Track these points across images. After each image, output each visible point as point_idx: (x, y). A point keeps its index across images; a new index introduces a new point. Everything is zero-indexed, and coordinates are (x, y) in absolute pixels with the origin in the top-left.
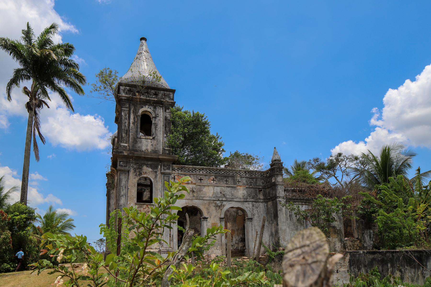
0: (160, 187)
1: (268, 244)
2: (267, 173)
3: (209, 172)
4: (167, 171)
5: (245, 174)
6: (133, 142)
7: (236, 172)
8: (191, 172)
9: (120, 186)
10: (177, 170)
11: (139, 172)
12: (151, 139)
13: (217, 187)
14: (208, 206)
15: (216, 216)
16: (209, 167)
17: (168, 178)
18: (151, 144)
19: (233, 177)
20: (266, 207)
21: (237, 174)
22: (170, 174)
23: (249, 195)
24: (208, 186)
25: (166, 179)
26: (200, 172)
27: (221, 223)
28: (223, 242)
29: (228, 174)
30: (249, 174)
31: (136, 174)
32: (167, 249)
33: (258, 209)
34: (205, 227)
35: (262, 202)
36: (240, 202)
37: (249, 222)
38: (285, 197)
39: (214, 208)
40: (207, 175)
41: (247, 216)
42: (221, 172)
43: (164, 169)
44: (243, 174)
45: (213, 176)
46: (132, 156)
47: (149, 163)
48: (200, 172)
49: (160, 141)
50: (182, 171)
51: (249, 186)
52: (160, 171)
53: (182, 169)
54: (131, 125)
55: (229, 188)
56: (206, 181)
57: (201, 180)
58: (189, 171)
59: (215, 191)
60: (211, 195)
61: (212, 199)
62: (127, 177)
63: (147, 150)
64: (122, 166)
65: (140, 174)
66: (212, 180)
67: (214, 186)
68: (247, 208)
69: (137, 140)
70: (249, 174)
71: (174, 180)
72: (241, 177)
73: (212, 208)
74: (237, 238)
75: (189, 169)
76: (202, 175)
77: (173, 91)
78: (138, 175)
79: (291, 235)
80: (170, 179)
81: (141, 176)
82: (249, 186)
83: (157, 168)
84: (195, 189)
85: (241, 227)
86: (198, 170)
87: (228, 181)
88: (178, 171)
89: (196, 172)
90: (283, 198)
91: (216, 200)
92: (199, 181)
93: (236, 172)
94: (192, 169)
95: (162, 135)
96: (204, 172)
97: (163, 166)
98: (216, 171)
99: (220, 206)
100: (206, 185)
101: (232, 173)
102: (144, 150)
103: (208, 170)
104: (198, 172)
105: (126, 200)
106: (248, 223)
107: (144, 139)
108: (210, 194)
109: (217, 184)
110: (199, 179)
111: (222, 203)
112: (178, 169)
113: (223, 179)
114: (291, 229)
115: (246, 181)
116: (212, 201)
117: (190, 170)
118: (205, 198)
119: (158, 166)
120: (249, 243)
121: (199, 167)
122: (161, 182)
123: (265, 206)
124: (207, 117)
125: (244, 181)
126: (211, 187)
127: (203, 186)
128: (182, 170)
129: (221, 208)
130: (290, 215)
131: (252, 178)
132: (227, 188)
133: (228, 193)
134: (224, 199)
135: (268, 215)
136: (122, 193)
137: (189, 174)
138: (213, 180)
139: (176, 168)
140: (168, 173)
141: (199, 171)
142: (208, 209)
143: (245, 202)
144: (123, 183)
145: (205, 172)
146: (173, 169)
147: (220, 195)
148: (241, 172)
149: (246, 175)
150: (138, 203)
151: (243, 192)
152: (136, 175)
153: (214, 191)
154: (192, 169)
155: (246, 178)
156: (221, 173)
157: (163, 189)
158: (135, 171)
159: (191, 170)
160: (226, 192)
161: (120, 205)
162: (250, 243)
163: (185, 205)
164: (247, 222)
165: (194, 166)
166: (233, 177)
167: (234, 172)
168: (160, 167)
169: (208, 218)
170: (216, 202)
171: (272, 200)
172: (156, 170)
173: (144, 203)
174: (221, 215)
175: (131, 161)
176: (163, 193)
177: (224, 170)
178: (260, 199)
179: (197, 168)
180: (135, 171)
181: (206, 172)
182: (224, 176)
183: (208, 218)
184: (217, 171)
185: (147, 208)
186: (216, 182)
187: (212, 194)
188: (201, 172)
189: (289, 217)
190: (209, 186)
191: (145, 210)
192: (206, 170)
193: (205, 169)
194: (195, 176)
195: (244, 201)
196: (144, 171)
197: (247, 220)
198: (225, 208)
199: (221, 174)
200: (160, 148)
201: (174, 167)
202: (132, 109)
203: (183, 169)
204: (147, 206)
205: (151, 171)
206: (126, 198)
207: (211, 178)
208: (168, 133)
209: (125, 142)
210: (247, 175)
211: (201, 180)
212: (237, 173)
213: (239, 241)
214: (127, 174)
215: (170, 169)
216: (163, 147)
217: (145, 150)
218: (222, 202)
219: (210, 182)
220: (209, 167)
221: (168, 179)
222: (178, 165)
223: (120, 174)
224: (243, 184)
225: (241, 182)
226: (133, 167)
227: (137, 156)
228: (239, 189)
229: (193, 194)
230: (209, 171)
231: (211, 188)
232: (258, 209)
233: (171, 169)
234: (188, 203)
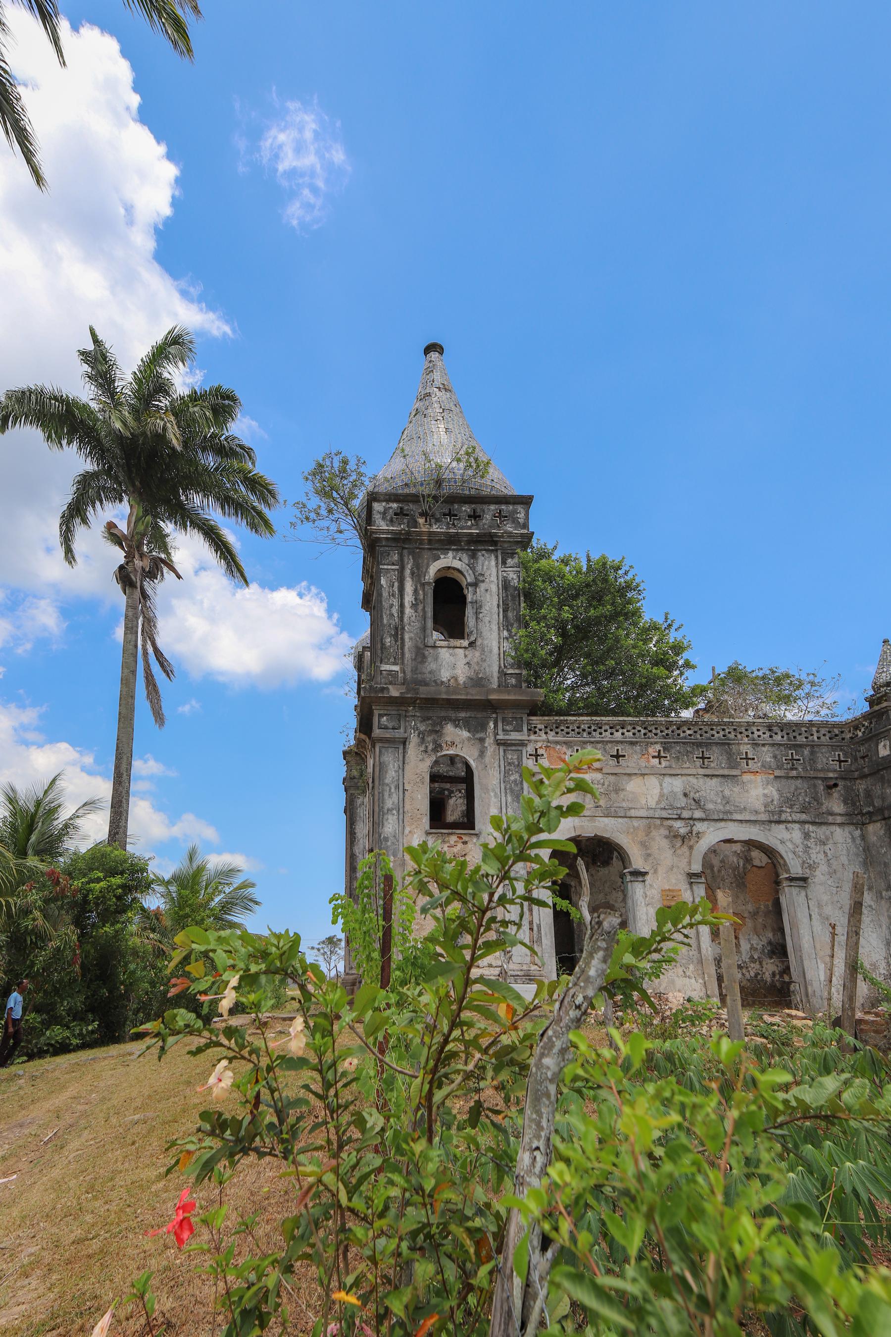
0: (495, 782)
2: (856, 728)
4: (515, 736)
5: (768, 734)
6: (415, 659)
7: (735, 730)
8: (585, 734)
9: (383, 784)
11: (435, 742)
12: (465, 648)
13: (673, 778)
14: (647, 836)
18: (465, 661)
19: (725, 744)
21: (739, 736)
22: (522, 744)
23: (789, 802)
24: (643, 775)
28: (704, 951)
29: (708, 735)
30: (784, 733)
31: (427, 747)
36: (755, 821)
37: (795, 891)
39: (665, 843)
40: (637, 742)
41: (788, 871)
43: (503, 730)
44: (760, 733)
45: (656, 743)
46: (411, 698)
47: (463, 715)
49: (491, 651)
50: (557, 733)
51: (788, 773)
52: (492, 738)
53: (557, 728)
54: (408, 611)
55: (715, 780)
56: (634, 760)
57: (617, 756)
58: (579, 733)
59: (665, 791)
60: (652, 803)
62: (401, 759)
63: (456, 679)
64: (386, 728)
65: (438, 747)
67: (661, 775)
68: (782, 842)
69: (427, 653)
70: (784, 733)
72: (755, 745)
73: (660, 842)
74: (754, 942)
75: (578, 728)
76: (622, 742)
77: (526, 501)
78: (433, 750)
80: (524, 759)
81: (439, 754)
82: (788, 773)
83: (483, 727)
85: (767, 906)
86: (607, 727)
87: (709, 758)
88: (546, 733)
89: (601, 734)
91: (671, 816)
92: (613, 762)
93: (735, 730)
94: (589, 728)
95: (495, 635)
96: (627, 734)
99: (683, 838)
100: (637, 772)
101: (722, 733)
102: (444, 679)
104: (608, 734)
105: (401, 822)
106: (791, 894)
107: (445, 649)
108: (650, 799)
109: (670, 767)
110: (612, 756)
111: (692, 826)
112: (546, 727)
113: (691, 752)
115: (775, 757)
116: (658, 822)
117: (584, 730)
118: (633, 811)
119: (488, 723)
120: (802, 961)
121: (610, 718)
122: (497, 768)
124: (631, 567)
125: (767, 755)
126: (652, 777)
127: (625, 774)
128: (558, 730)
129: (691, 843)
131: (798, 747)
132: (708, 780)
133: (712, 796)
134: (698, 814)
136: (389, 803)
137: (581, 741)
138: (659, 757)
139: (539, 726)
141: (609, 731)
142: (644, 845)
143: (773, 825)
144: (391, 774)
145: (630, 734)
146: (530, 730)
147: (682, 802)
148: (755, 729)
149: (771, 736)
150: (433, 831)
151: (766, 791)
152: (426, 751)
153: (662, 789)
155: (773, 745)
157: (505, 789)
158: (423, 739)
160: (702, 793)
161: (384, 837)
162: (806, 963)
164: (786, 889)
165: (594, 718)
166: (725, 744)
167: (727, 731)
168: (492, 726)
171: (884, 819)
172: (482, 735)
173: (450, 831)
174: (689, 863)
175: (411, 714)
177: (693, 725)
180: (423, 739)
182: (693, 743)
185: (460, 846)
186: (668, 763)
187: (656, 798)
188: (618, 735)
191: (455, 850)
193: (630, 724)
195: (771, 822)
196: (449, 739)
197: (785, 883)
198: (701, 842)
200: (492, 669)
202: (409, 566)
203: (562, 728)
204: (461, 838)
205: (469, 739)
206: (398, 819)
207: (650, 750)
208: (512, 625)
209: (392, 660)
210: (778, 738)
211: (617, 756)
212: (741, 733)
213: (763, 952)
214: (401, 751)
215: (522, 731)
216: (500, 667)
217: (449, 680)
218: (691, 822)
219: (648, 761)
221: (518, 758)
222: (546, 718)
223: (380, 751)
224: (763, 766)
225: (753, 759)
226: (416, 728)
227: (426, 699)
228: (750, 782)
231: (653, 781)
233: (525, 729)
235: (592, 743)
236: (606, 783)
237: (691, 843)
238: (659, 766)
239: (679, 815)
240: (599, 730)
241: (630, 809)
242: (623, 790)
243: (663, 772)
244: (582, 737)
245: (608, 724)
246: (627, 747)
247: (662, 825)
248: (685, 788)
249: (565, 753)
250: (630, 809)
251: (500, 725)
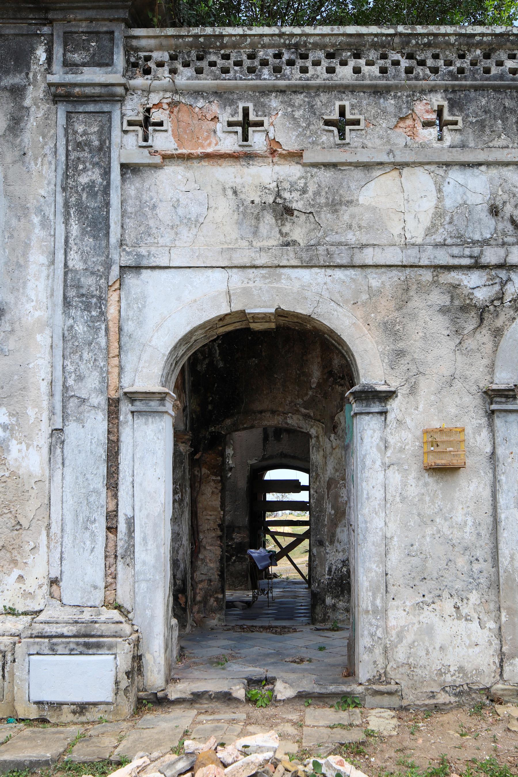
3: (409, 71)
8: (266, 72)
10: (166, 68)
13: (469, 171)
14: (400, 309)
15: (453, 377)
16: (401, 29)
17: (102, 127)
25: (85, 133)
26: (339, 69)
27: (491, 425)
32: (87, 616)
34: (368, 462)
42: (500, 64)
45: (433, 90)
48: (339, 69)
50: (199, 71)
53: (200, 58)
58: (251, 70)
59: (448, 203)
61: (425, 262)
66: (427, 124)
71: (146, 139)
80: (116, 133)
84: (296, 195)
86: (320, 54)
88: (173, 71)
89: (304, 70)
91: (456, 262)
94: (278, 56)
97: (65, 45)
98: (462, 57)
100: (384, 158)
103: (397, 57)
104: (321, 70)
108: (411, 224)
109: (463, 146)
110: (327, 123)
111: (503, 284)
112: (173, 58)
116: (427, 276)
117: (264, 63)
127: (357, 165)
128: (204, 64)
129: (499, 323)
137: (255, 89)
139: (157, 55)
140: (97, 90)
141: (325, 63)
153: (440, 199)
154: (278, 56)
156: (494, 70)
159: (271, 60)
163: (224, 310)
169: (390, 395)
170: (454, 277)
172: (17, 79)
174: (492, 368)
176: (61, 229)
179: (316, 46)
181: (383, 70)
183: (390, 395)
184: (469, 57)
186: (458, 138)
187: (426, 221)
190: (406, 164)
192: (384, 56)
193: (374, 46)
194: (299, 99)
199: (501, 77)
201: (143, 43)
203: (213, 58)
207: (420, 108)
215: (109, 64)
218: (503, 274)
219: (413, 135)
220: (401, 29)
221: (100, 133)
222: (171, 31)
229: (285, 230)
230: (405, 63)
234: (244, 289)
235: (282, 91)
236: (312, 188)
237: (499, 323)
238: (437, 145)
239: (477, 258)
240: (300, 63)
241: (363, 246)
242: (350, 202)
243: (446, 158)
244: (259, 77)
245: (323, 47)
246: (366, 100)
247: (435, 282)
248: (494, 195)
249: (215, 119)
250: (363, 246)
251: (58, 51)
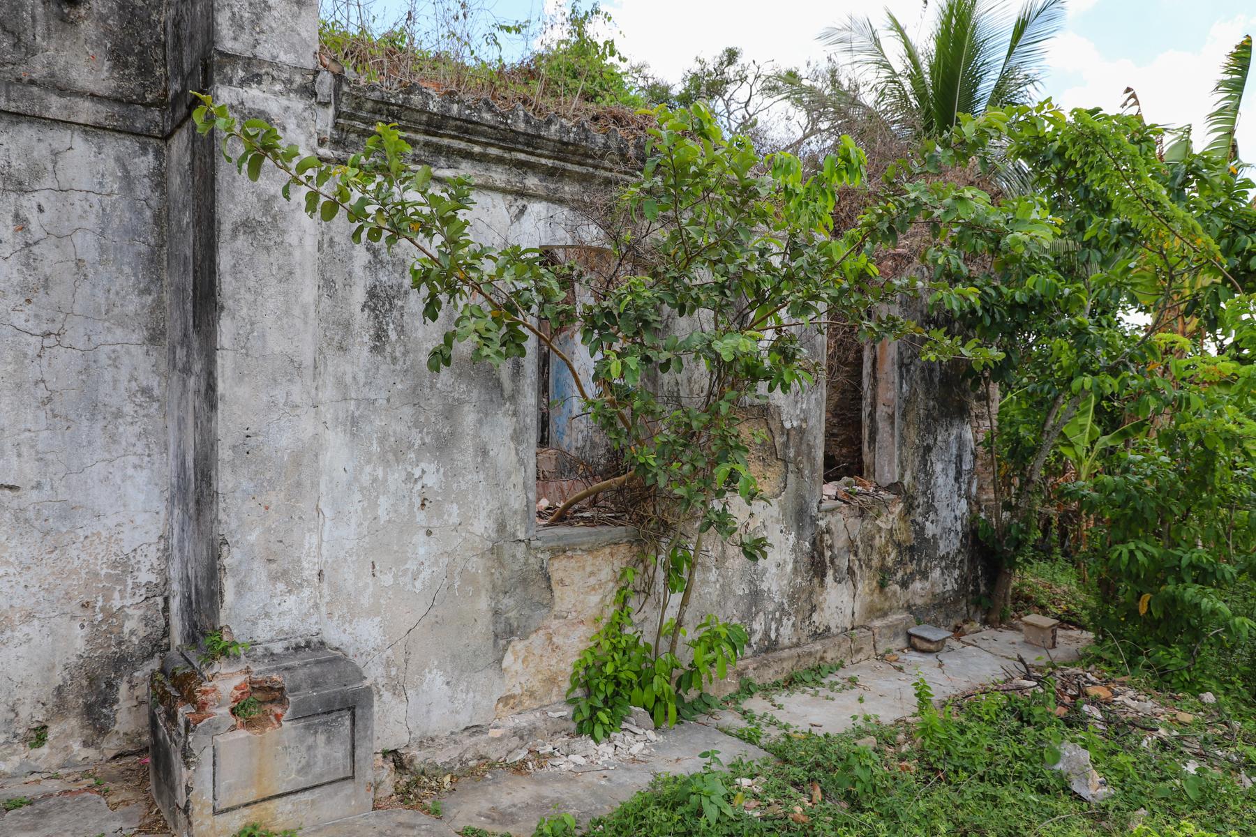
1: (144, 577)
20: (143, 189)
33: (28, 204)
35: (92, 129)
38: (326, 79)
79: (375, 505)
90: (308, 91)
114: (382, 440)
123: (128, 181)
130: (372, 294)
135: (166, 279)
178: (64, 90)
189: (361, 319)
232: (39, 198)
